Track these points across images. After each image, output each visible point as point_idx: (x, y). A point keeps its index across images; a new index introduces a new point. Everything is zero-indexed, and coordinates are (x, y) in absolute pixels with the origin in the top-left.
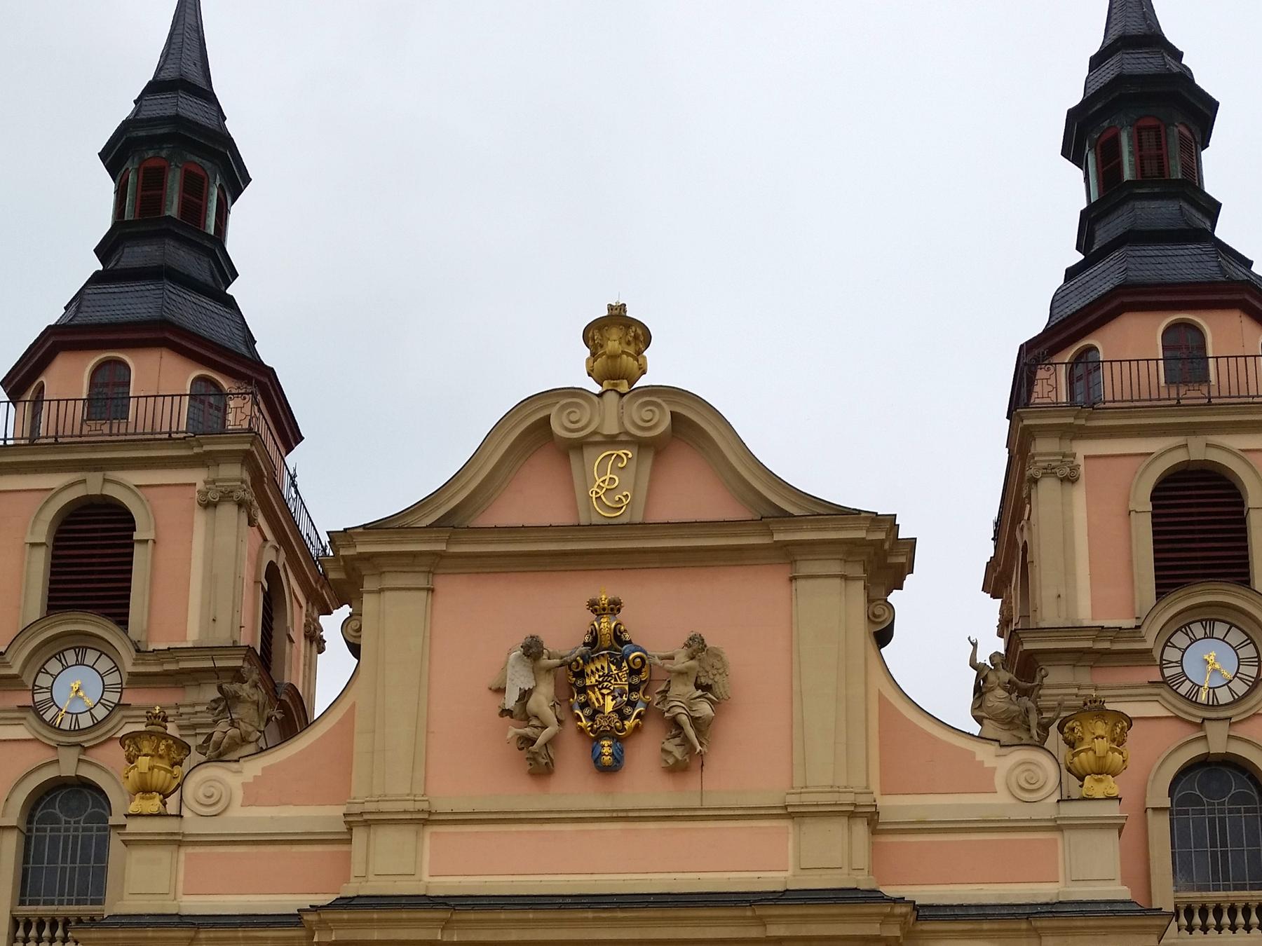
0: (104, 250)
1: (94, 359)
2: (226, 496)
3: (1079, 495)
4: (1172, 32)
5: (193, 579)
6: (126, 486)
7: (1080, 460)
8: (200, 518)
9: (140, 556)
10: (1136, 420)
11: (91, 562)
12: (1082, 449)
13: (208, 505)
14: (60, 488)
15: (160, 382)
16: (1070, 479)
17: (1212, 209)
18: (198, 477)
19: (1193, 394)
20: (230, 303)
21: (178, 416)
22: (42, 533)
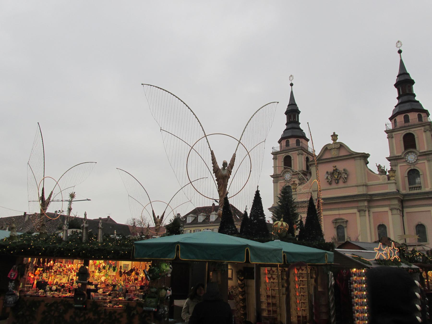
0: (286, 124)
1: (286, 140)
2: (300, 154)
3: (394, 139)
4: (408, 72)
5: (299, 163)
6: (290, 154)
7: (394, 136)
8: (298, 156)
9: (292, 161)
10: (401, 128)
11: (288, 162)
12: (394, 133)
13: (298, 155)
14: (284, 155)
15: (292, 142)
16: (392, 138)
17: (414, 95)
18: (297, 152)
19: (407, 124)
20: (299, 129)
21: (295, 146)
22: (283, 160)
